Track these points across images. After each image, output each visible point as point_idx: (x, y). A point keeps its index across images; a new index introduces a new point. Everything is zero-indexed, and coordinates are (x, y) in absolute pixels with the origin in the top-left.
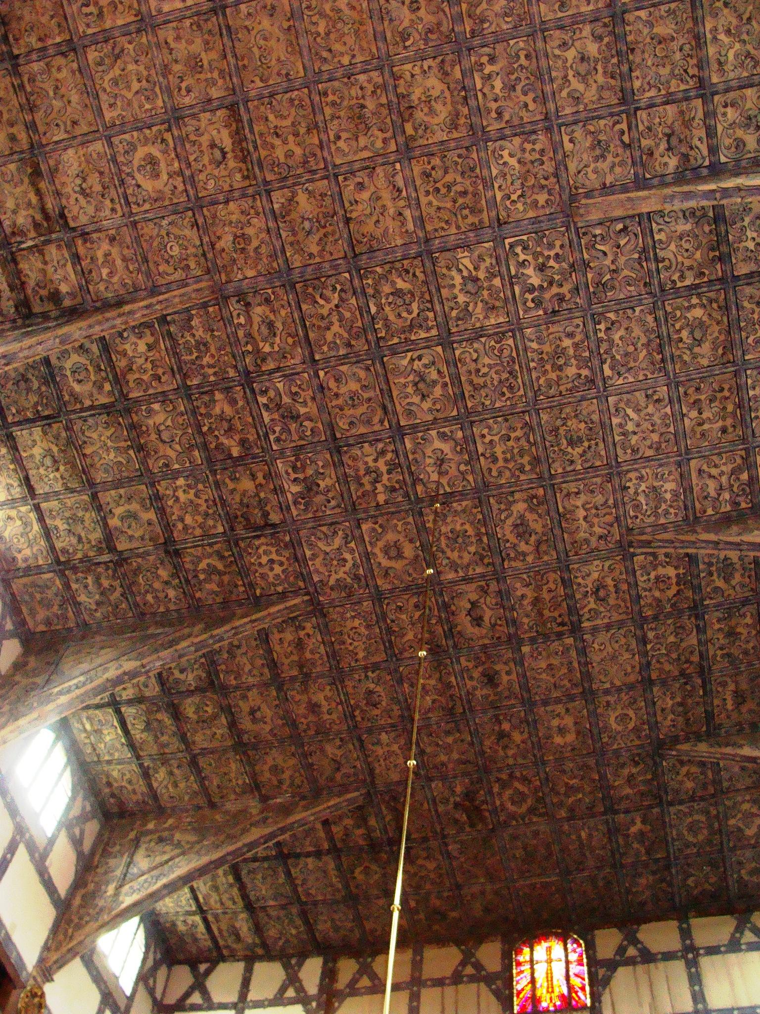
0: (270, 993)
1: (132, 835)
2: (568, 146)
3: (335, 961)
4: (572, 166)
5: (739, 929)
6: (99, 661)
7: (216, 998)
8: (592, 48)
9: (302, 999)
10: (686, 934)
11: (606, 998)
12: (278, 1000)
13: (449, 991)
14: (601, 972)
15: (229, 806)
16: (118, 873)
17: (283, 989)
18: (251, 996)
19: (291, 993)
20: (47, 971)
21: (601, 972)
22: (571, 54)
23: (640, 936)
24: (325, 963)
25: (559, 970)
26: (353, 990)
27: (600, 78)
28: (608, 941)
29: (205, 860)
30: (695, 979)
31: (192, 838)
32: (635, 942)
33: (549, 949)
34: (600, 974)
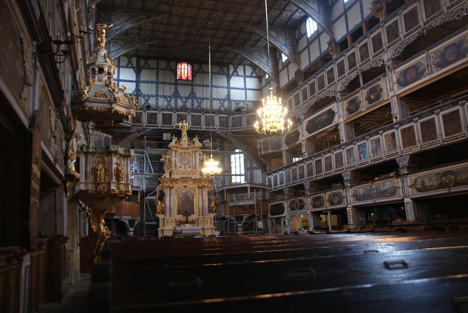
0: (125, 64)
3: (139, 59)
5: (220, 70)
6: (122, 21)
9: (132, 67)
11: (195, 79)
12: (127, 67)
13: (165, 71)
14: (194, 73)
15: (130, 36)
17: (128, 64)
19: (130, 65)
21: (194, 73)
23: (202, 67)
24: (137, 59)
25: (186, 71)
28: (197, 67)
29: (128, 51)
31: (124, 44)
32: (201, 68)
33: (184, 66)
34: (194, 73)
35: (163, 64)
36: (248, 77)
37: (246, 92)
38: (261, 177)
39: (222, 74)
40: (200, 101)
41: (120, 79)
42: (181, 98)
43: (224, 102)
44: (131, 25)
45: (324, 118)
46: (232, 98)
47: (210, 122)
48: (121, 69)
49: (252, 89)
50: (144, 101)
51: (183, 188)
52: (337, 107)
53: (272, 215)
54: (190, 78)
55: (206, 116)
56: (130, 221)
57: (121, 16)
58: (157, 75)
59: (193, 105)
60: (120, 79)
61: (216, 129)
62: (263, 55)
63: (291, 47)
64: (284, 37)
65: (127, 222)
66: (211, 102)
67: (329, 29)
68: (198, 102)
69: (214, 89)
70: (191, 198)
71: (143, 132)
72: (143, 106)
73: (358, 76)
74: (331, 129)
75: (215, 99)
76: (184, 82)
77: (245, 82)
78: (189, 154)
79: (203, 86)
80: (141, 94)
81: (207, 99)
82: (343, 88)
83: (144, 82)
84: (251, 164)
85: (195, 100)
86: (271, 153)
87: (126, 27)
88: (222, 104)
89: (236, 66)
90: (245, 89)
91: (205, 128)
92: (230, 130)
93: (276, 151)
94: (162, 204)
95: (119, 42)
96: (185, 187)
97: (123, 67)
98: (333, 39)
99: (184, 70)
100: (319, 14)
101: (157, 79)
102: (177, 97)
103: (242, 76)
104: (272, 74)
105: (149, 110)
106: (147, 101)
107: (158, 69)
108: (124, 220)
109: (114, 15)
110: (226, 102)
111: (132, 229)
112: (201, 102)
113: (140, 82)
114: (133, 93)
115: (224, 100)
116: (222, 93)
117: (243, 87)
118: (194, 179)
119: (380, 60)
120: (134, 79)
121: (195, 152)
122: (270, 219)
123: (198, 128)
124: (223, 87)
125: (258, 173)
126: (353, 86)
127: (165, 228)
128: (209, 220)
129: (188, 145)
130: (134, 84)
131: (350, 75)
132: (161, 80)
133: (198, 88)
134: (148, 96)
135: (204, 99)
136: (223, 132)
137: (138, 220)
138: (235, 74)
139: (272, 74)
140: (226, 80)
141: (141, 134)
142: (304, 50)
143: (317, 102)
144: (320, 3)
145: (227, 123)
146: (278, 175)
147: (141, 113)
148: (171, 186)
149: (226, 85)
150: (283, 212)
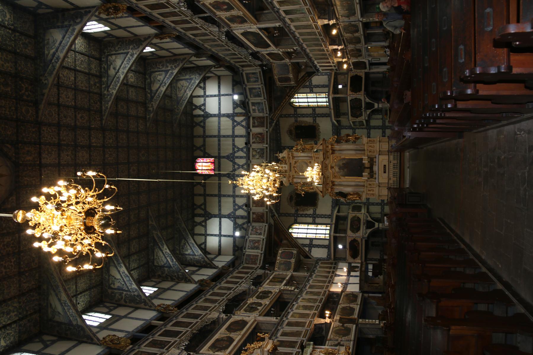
0: (203, 229)
1: (180, 256)
2: (93, 126)
4: (97, 126)
7: (203, 241)
8: (80, 115)
10: (199, 137)
11: (213, 155)
12: (205, 227)
16: (191, 257)
17: (203, 226)
18: (204, 233)
19: (204, 224)
20: (215, 267)
22: (80, 120)
25: (204, 164)
26: (205, 210)
27: (84, 115)
30: (211, 136)
33: (199, 166)
34: (206, 155)
35: (199, 190)
36: (205, 92)
37: (223, 95)
38: (322, 77)
39: (205, 123)
40: (236, 149)
41: (218, 233)
42: (234, 170)
43: (236, 121)
44: (165, 247)
45: (251, 38)
46: (230, 111)
47: (260, 138)
48: (208, 233)
49: (219, 87)
50: (240, 210)
51: (333, 170)
52: (238, 30)
53: (366, 68)
54: (212, 160)
55: (253, 143)
56: (368, 228)
57: (157, 256)
58: (212, 195)
59: (241, 157)
60: (218, 233)
61: (267, 132)
62: (179, 85)
63: (168, 64)
64: (158, 73)
65: (369, 231)
66: (237, 136)
67: (143, 41)
68: (238, 151)
69: (223, 133)
70: (344, 162)
71: (274, 211)
72: (246, 211)
73: (199, 18)
74: (266, 33)
75: (233, 132)
76: (217, 166)
77: (211, 96)
78: (296, 162)
79: (219, 145)
80: (232, 212)
81: (234, 141)
82: (215, 26)
83: (220, 210)
84: (306, 87)
85: (236, 155)
86: (293, 76)
87: (168, 251)
88: (239, 124)
89: (194, 107)
90: (219, 95)
91: (267, 144)
92: (267, 115)
93: (290, 69)
94: (351, 195)
95: (182, 244)
96: (332, 167)
97: (206, 231)
98: (156, 36)
99: (204, 166)
100: (127, 53)
101: (215, 196)
102: (234, 174)
103: (205, 100)
104: (200, 75)
105: (249, 205)
106: (240, 207)
107: (205, 195)
108: (367, 235)
109: (157, 263)
110: (237, 119)
111: (377, 224)
112: (238, 148)
113: (220, 214)
114: (232, 221)
115: (234, 121)
116: (226, 123)
117: (217, 98)
118: (324, 159)
119: (178, 3)
120: (217, 220)
121: (293, 157)
122: (370, 69)
123: (267, 151)
124: (219, 123)
125: (316, 80)
126: (211, 20)
127: (377, 193)
128: (370, 145)
129: (286, 164)
130: (223, 220)
131: (198, 22)
132: (216, 192)
133: (222, 151)
134: (234, 206)
135: (234, 145)
136: (270, 124)
137: (367, 217)
138: (203, 108)
139: (200, 75)
140: (211, 119)
141: (276, 214)
142: (170, 52)
143: (232, 42)
144: (114, 52)
145: (260, 118)
146: (318, 65)
147: (253, 213)
148: (331, 185)
149: (217, 119)
150: (365, 63)
